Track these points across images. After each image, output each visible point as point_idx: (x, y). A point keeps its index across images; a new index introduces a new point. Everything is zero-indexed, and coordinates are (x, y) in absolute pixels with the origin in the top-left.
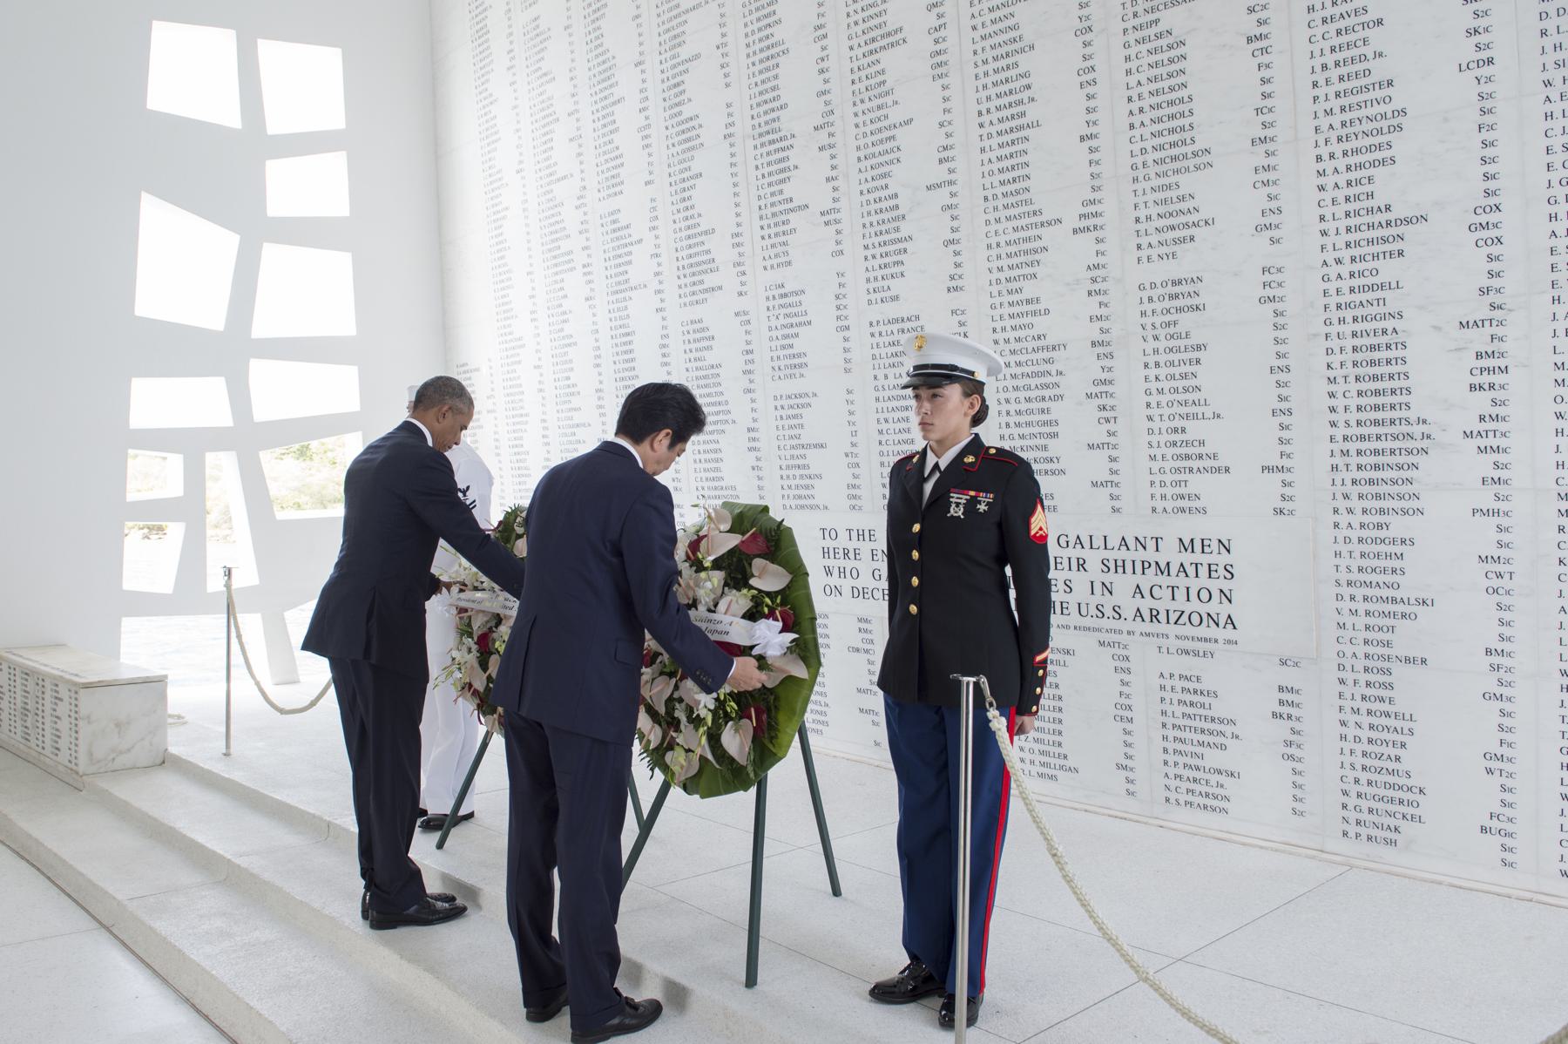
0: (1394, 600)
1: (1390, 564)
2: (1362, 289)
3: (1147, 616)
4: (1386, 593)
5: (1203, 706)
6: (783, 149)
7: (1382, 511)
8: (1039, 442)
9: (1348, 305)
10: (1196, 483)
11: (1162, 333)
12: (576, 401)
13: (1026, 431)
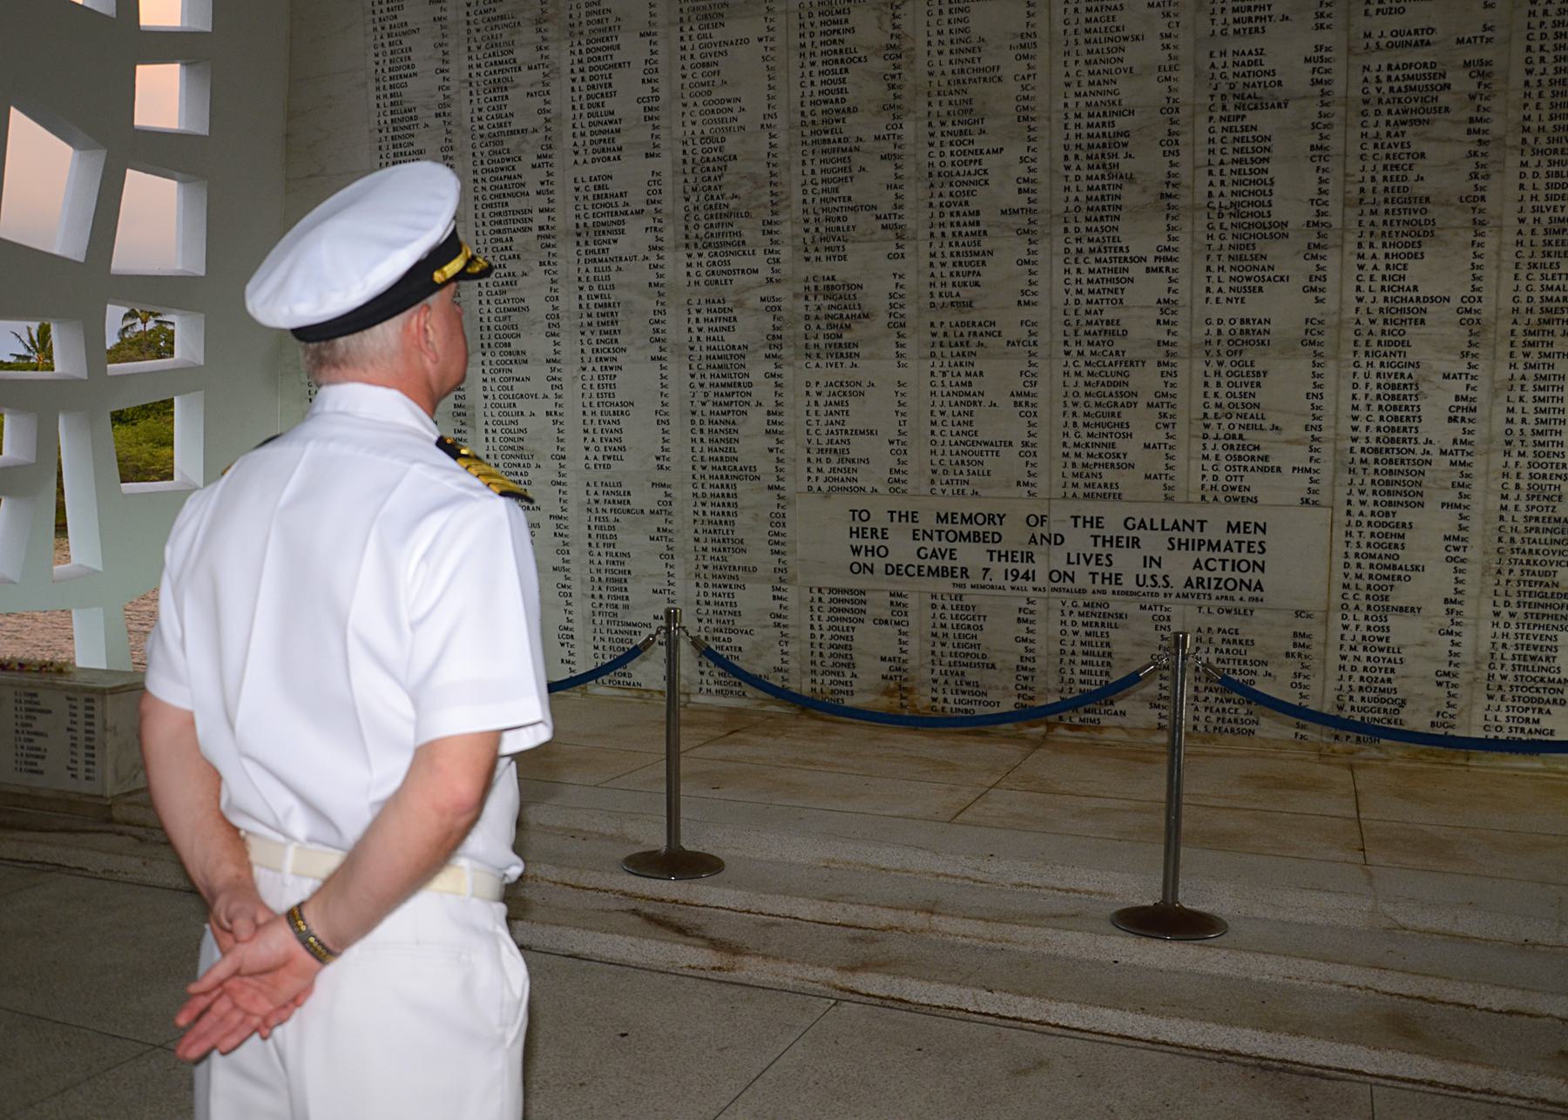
0: (1394, 567)
1: (1394, 541)
2: (1388, 343)
3: (1194, 582)
4: (1388, 562)
5: (1239, 652)
6: (844, 150)
7: (1390, 504)
8: (1105, 440)
9: (1374, 354)
10: (1250, 479)
11: (1227, 361)
12: (518, 370)
13: (1096, 431)
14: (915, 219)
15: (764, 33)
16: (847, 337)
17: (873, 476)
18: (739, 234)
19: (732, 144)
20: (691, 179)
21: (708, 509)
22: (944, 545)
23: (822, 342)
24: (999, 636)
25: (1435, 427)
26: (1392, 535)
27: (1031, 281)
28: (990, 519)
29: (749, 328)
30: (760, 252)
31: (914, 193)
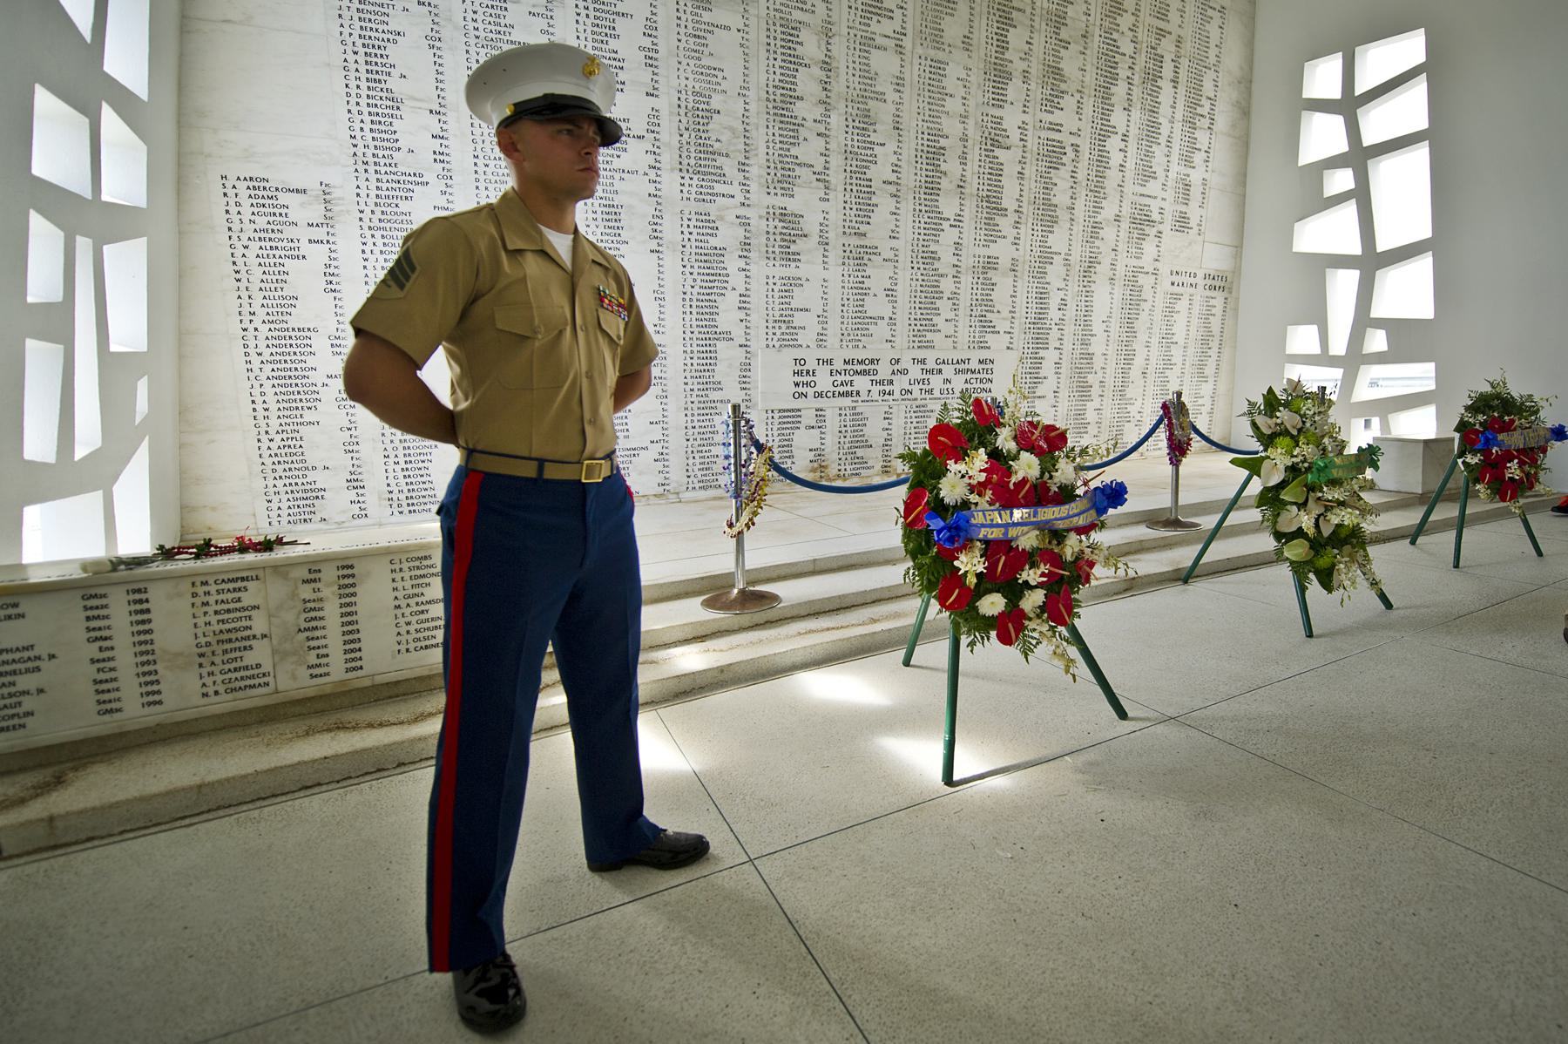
14: (836, 178)
15: (741, 27)
16: (793, 248)
17: (807, 337)
18: (721, 168)
19: (716, 102)
20: (684, 120)
21: (695, 361)
22: (848, 378)
23: (777, 250)
24: (874, 430)
25: (1054, 314)
26: (1038, 362)
27: (894, 224)
28: (872, 362)
29: (728, 236)
30: (736, 183)
31: (836, 161)
